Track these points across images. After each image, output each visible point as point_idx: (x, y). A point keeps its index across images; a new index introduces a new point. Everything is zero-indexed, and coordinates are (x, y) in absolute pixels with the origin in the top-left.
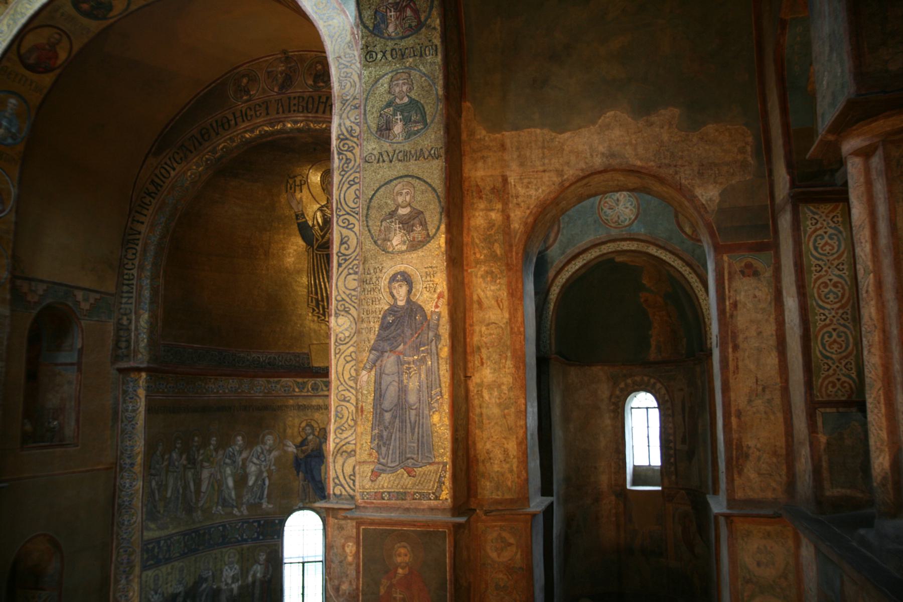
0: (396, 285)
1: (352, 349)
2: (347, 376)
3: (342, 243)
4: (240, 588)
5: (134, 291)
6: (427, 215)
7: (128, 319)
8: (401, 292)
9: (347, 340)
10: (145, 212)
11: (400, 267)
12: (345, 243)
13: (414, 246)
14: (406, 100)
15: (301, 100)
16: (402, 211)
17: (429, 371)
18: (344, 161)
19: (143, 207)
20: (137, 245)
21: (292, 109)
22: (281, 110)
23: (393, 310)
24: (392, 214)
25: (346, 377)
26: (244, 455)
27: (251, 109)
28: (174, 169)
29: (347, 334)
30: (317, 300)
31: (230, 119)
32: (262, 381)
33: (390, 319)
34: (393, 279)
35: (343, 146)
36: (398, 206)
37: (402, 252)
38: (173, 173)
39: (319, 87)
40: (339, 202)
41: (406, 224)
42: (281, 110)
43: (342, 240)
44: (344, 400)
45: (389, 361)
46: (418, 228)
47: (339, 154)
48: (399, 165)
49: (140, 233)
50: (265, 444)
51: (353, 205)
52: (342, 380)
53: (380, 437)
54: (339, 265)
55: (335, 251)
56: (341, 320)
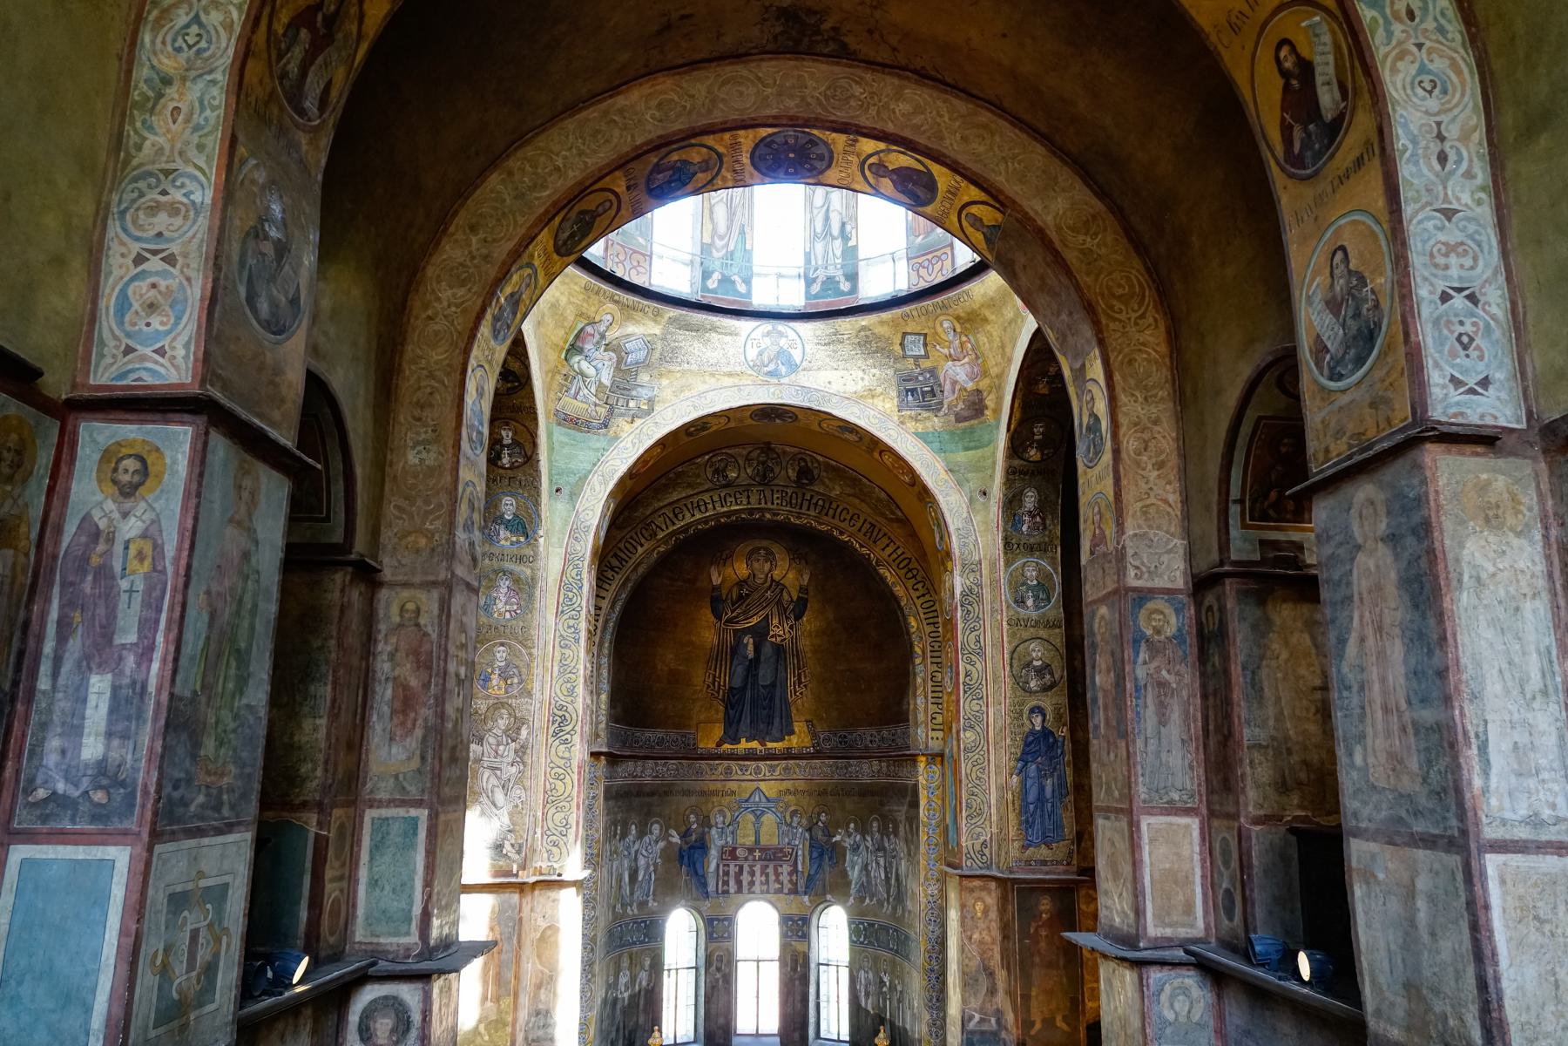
2: (974, 776)
3: (967, 676)
4: (631, 997)
8: (1038, 720)
10: (607, 587)
11: (1034, 703)
13: (1046, 689)
14: (1035, 582)
16: (1036, 663)
17: (1059, 777)
23: (1032, 732)
24: (1029, 664)
26: (636, 847)
28: (642, 545)
30: (714, 677)
32: (650, 763)
33: (1031, 738)
34: (1032, 711)
37: (1036, 692)
38: (640, 550)
40: (963, 643)
41: (1040, 672)
46: (1048, 677)
50: (651, 833)
53: (1027, 821)
54: (965, 692)
56: (968, 734)
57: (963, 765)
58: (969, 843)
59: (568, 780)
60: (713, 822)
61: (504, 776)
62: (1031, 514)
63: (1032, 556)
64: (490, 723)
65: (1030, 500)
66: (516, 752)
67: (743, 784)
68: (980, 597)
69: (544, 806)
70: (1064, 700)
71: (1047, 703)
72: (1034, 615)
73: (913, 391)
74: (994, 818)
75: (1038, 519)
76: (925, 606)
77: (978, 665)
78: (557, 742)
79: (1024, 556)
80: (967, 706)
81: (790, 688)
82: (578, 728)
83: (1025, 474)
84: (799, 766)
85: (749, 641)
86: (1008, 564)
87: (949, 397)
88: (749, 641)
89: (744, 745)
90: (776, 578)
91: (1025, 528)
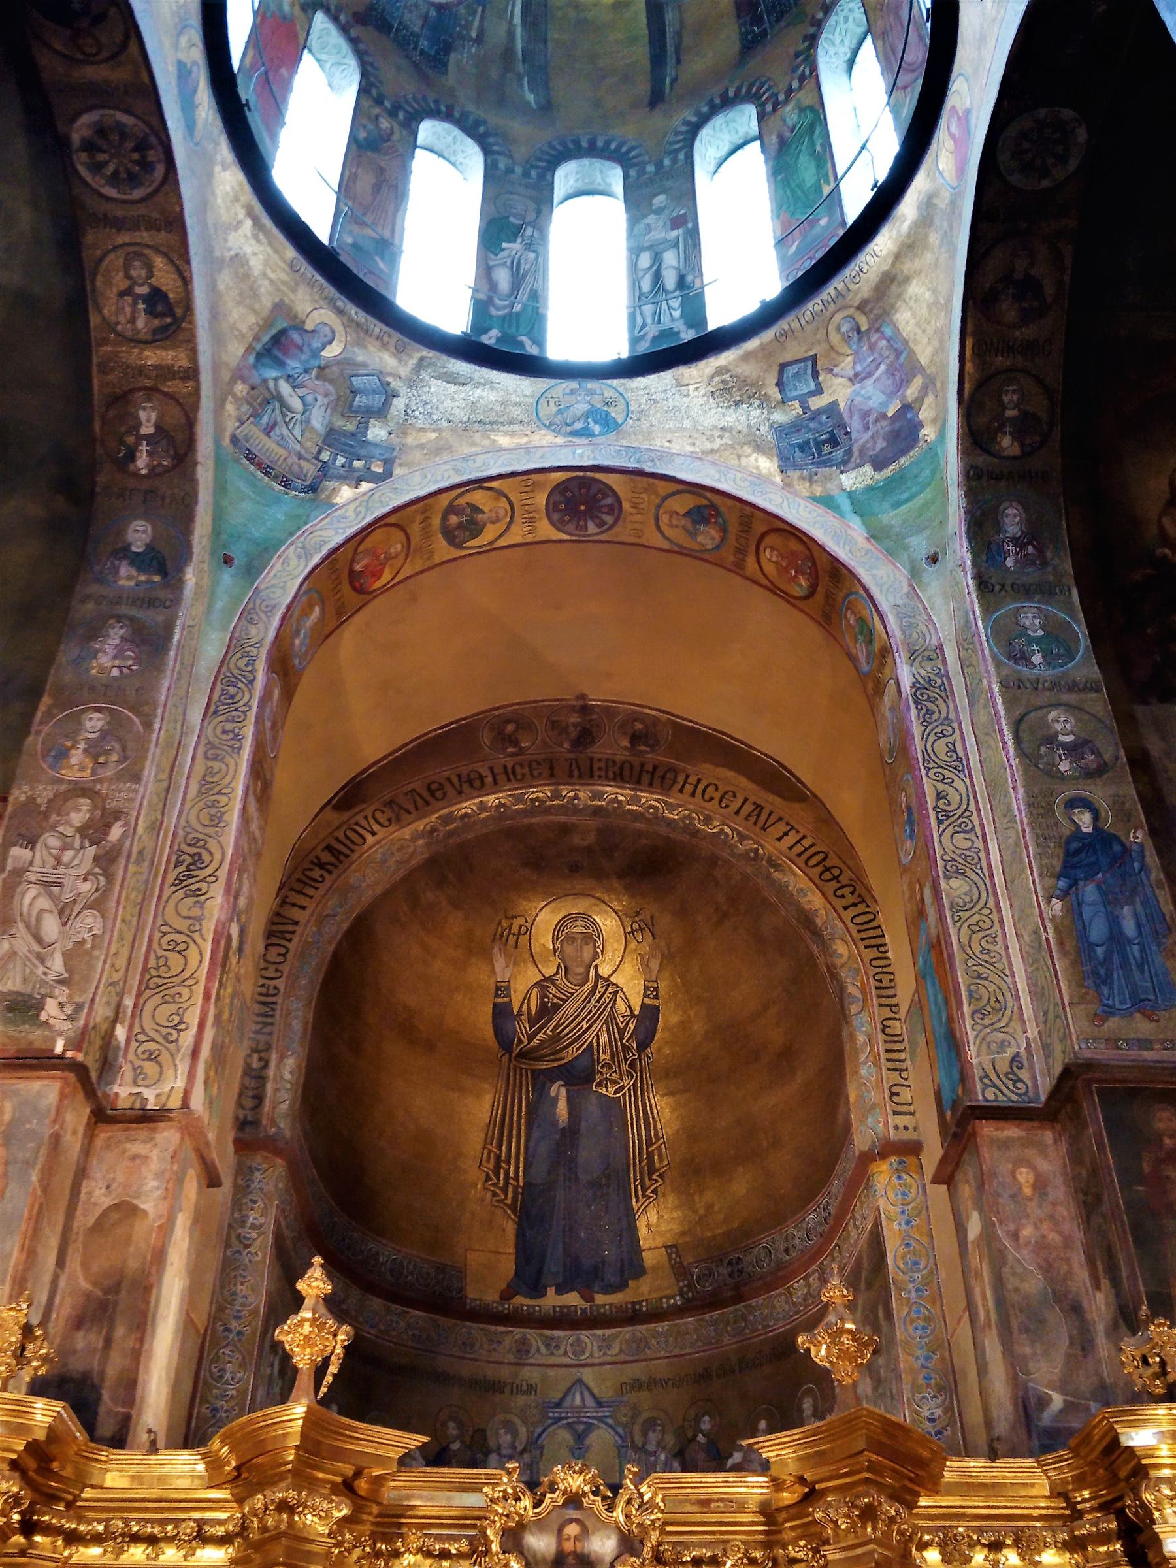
0: (1076, 811)
1: (977, 917)
2: (977, 949)
3: (939, 797)
5: (278, 1013)
6: (1098, 744)
7: (260, 1059)
9: (969, 906)
12: (944, 798)
13: (1091, 774)
15: (610, 763)
18: (924, 711)
19: (306, 884)
20: (290, 941)
21: (596, 773)
22: (576, 773)
25: (977, 951)
27: (522, 766)
29: (967, 899)
31: (484, 774)
35: (922, 695)
36: (1057, 734)
39: (641, 751)
42: (576, 773)
43: (938, 794)
44: (979, 977)
45: (1090, 891)
47: (916, 703)
48: (1047, 694)
49: (296, 923)
51: (946, 759)
52: (969, 951)
54: (940, 822)
55: (930, 805)
56: (954, 883)
57: (953, 932)
58: (986, 1059)
59: (193, 952)
60: (492, 1443)
61: (67, 896)
62: (1015, 541)
63: (1030, 599)
64: (54, 818)
65: (1012, 521)
66: (96, 859)
67: (551, 1372)
68: (947, 692)
69: (139, 995)
70: (1129, 790)
71: (1098, 793)
72: (1048, 673)
73: (803, 447)
74: (1028, 1012)
75: (1031, 549)
76: (858, 920)
77: (958, 783)
78: (181, 894)
79: (1014, 600)
80: (945, 843)
81: (635, 1186)
82: (223, 874)
83: (998, 478)
84: (656, 1334)
85: (559, 1093)
86: (987, 610)
87: (860, 437)
88: (559, 1093)
89: (552, 1300)
90: (605, 971)
91: (1010, 562)
